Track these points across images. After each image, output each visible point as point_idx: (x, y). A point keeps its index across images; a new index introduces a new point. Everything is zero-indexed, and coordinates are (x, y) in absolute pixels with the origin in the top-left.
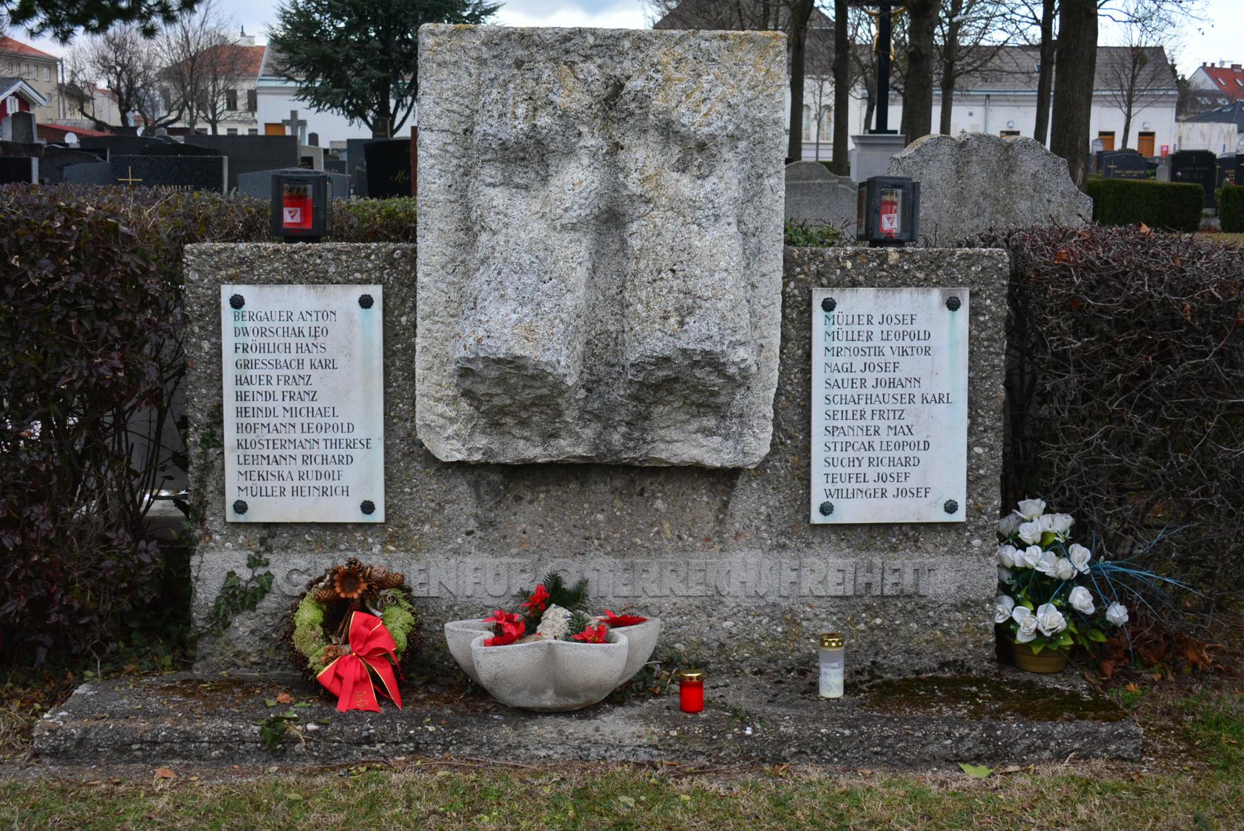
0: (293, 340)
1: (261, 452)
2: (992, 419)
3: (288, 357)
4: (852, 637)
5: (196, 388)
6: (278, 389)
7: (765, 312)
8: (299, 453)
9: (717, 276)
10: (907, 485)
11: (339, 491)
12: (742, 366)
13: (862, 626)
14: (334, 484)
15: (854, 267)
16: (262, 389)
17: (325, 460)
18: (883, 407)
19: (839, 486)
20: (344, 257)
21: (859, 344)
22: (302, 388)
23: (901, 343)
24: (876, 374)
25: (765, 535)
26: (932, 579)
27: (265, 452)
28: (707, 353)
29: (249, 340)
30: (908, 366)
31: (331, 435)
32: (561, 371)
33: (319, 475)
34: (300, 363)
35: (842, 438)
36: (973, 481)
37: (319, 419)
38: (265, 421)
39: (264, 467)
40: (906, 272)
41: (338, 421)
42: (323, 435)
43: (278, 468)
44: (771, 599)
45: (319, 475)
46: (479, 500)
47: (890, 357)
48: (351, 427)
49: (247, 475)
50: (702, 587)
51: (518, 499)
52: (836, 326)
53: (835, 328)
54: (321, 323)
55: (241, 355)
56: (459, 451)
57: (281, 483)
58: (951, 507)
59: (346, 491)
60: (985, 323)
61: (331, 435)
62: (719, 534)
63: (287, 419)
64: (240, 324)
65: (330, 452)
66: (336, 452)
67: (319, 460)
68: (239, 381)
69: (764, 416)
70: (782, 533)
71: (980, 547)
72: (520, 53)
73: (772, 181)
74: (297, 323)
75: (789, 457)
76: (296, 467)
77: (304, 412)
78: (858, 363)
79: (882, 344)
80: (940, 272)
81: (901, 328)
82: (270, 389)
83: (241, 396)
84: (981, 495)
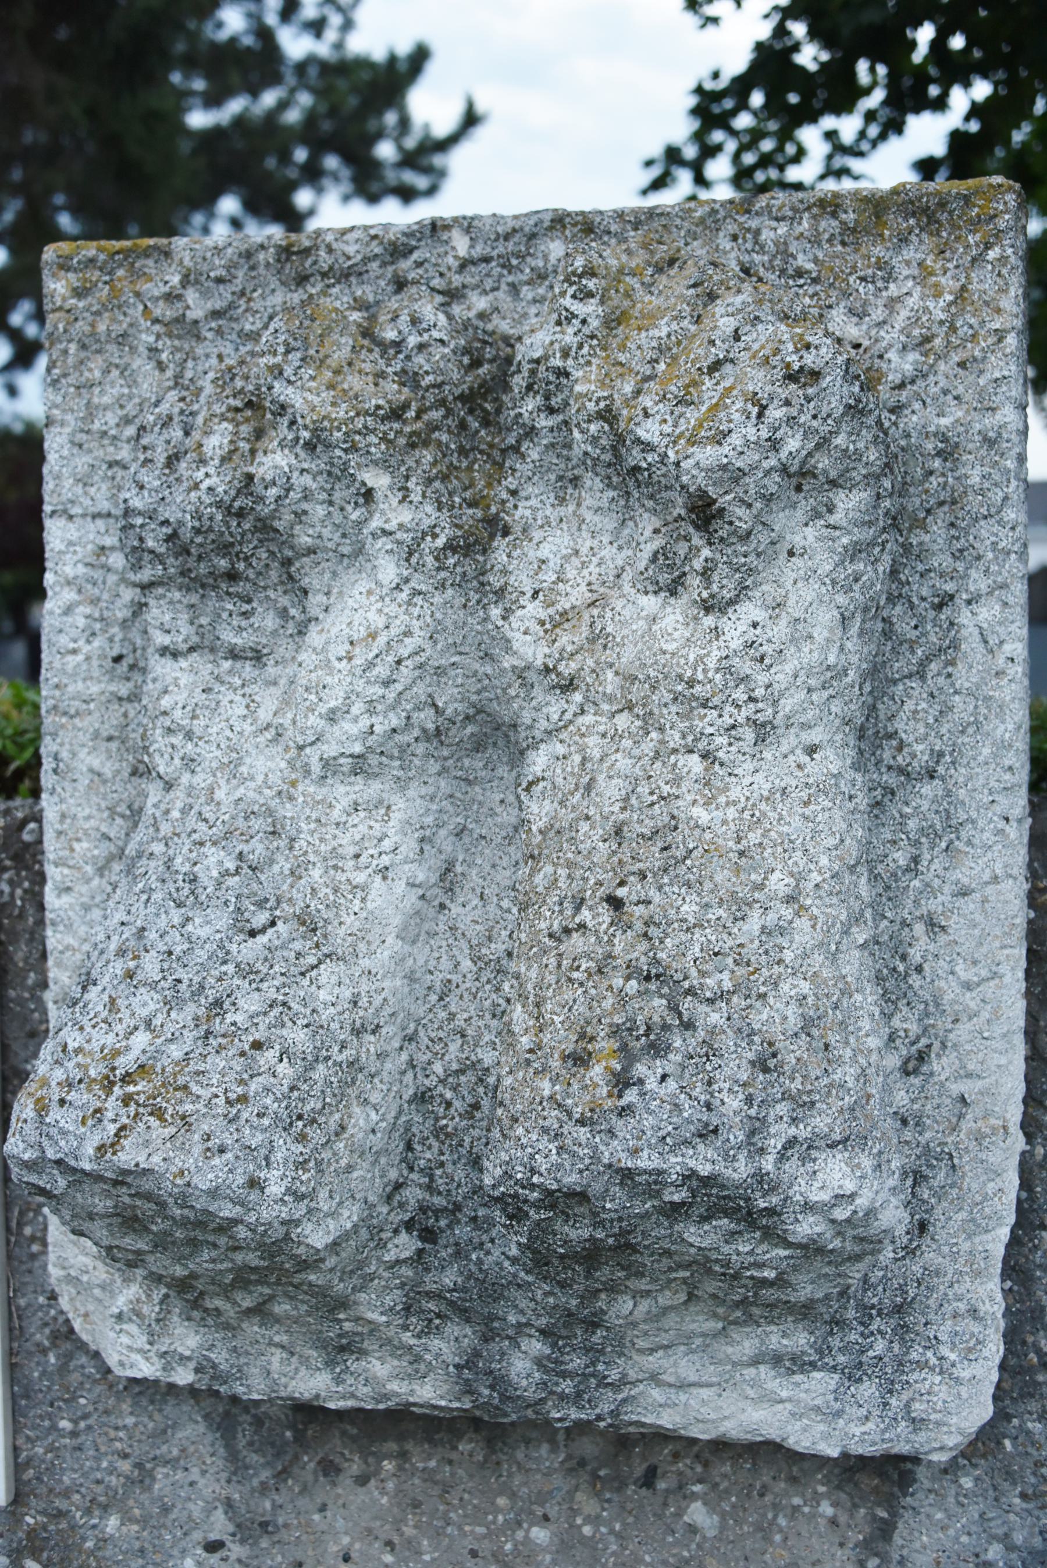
7: (970, 1000)
9: (754, 922)
12: (841, 1214)
46: (237, 1467)
51: (329, 1469)
73: (987, 613)
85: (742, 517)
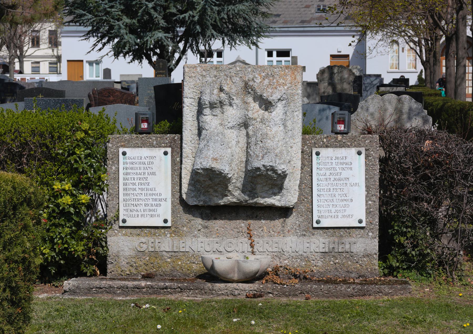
0: (142, 166)
1: (131, 203)
2: (376, 192)
3: (140, 171)
4: (328, 267)
5: (110, 182)
6: (137, 182)
7: (295, 155)
8: (143, 203)
10: (345, 214)
11: (156, 216)
12: (283, 171)
13: (332, 263)
14: (155, 213)
15: (327, 141)
16: (132, 182)
17: (152, 205)
18: (337, 187)
19: (322, 214)
20: (159, 139)
21: (328, 167)
22: (145, 181)
23: (342, 166)
24: (334, 177)
25: (298, 231)
26: (355, 247)
27: (132, 203)
28: (271, 166)
29: (128, 166)
30: (345, 174)
31: (154, 197)
32: (226, 172)
33: (150, 210)
34: (144, 173)
35: (323, 198)
36: (368, 212)
37: (150, 192)
38: (133, 192)
39: (132, 208)
40: (344, 143)
41: (156, 192)
42: (151, 197)
43: (137, 208)
44: (301, 253)
45: (150, 210)
47: (338, 171)
48: (160, 194)
49: (127, 210)
50: (277, 249)
52: (321, 160)
53: (320, 161)
54: (151, 160)
55: (125, 171)
56: (196, 201)
57: (137, 213)
58: (360, 222)
59: (159, 216)
60: (371, 159)
61: (154, 197)
62: (283, 230)
63: (140, 192)
64: (125, 161)
65: (153, 203)
66: (156, 203)
67: (150, 205)
68: (124, 179)
69: (295, 190)
70: (304, 230)
71: (372, 236)
72: (215, 73)
74: (143, 160)
75: (306, 205)
76: (142, 208)
77: (145, 189)
78: (328, 173)
79: (336, 166)
80: (356, 143)
81: (342, 161)
82: (134, 182)
83: (125, 184)
84: (371, 218)
85: (274, 104)
